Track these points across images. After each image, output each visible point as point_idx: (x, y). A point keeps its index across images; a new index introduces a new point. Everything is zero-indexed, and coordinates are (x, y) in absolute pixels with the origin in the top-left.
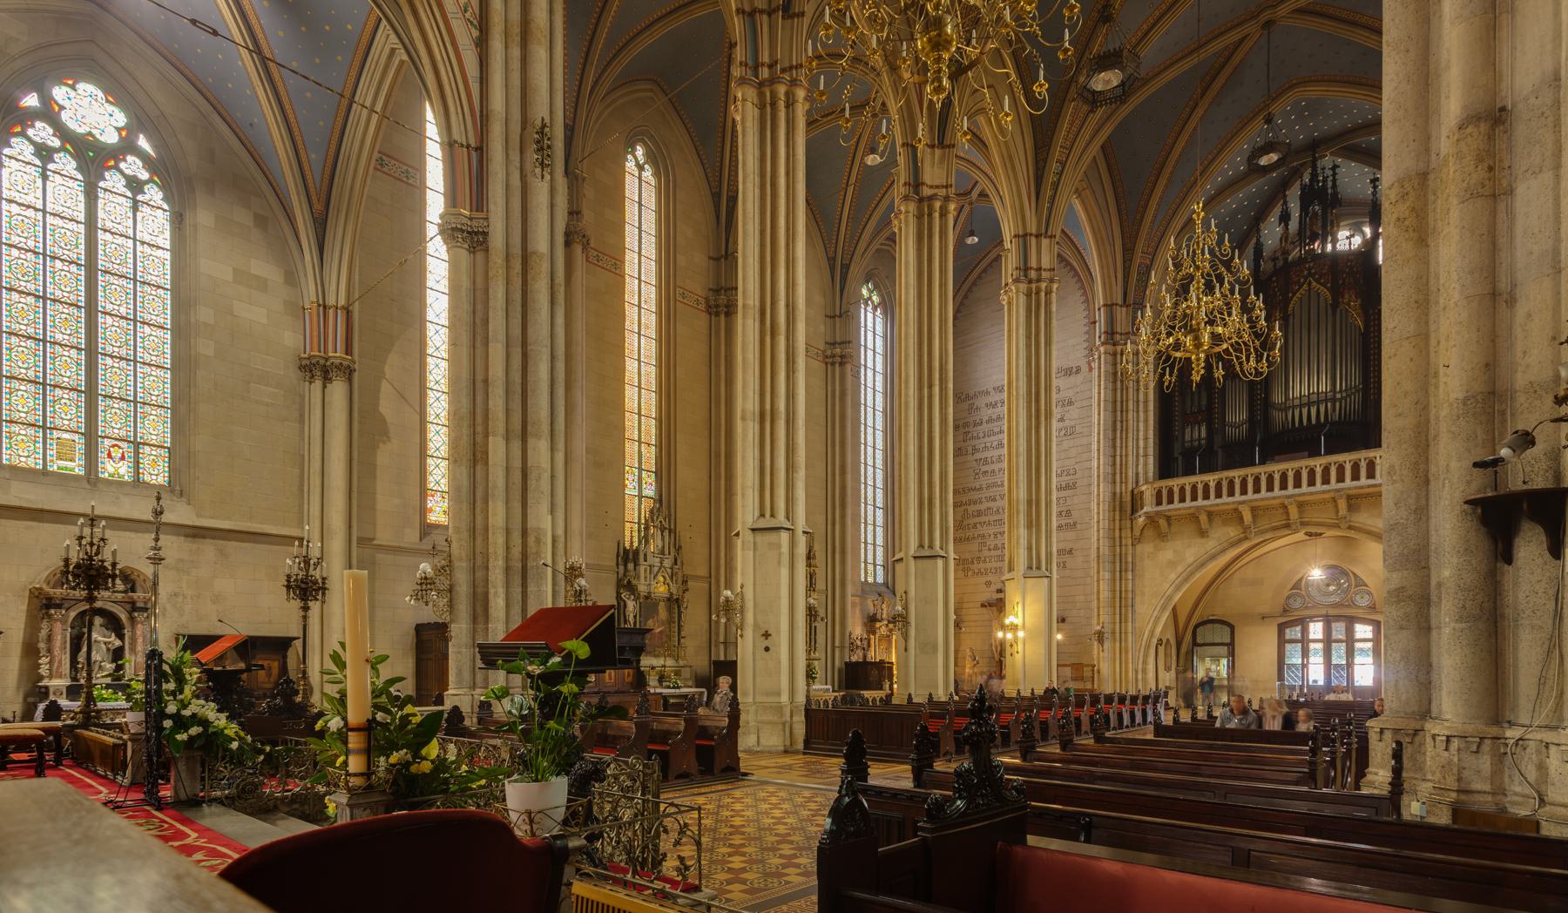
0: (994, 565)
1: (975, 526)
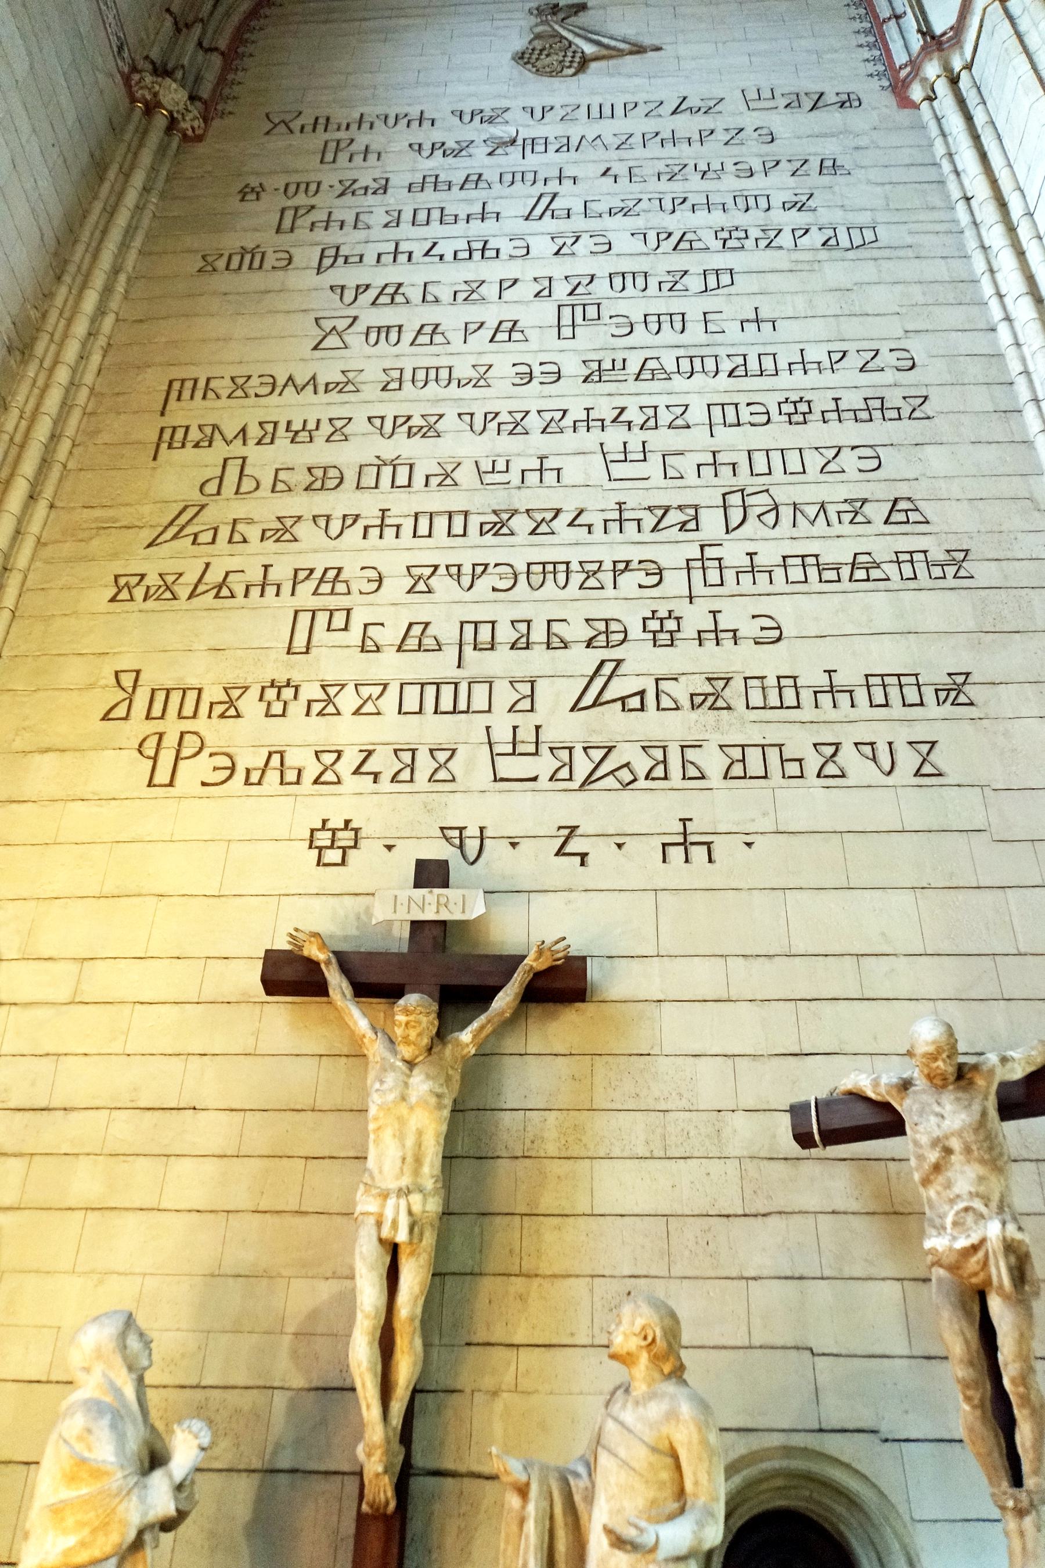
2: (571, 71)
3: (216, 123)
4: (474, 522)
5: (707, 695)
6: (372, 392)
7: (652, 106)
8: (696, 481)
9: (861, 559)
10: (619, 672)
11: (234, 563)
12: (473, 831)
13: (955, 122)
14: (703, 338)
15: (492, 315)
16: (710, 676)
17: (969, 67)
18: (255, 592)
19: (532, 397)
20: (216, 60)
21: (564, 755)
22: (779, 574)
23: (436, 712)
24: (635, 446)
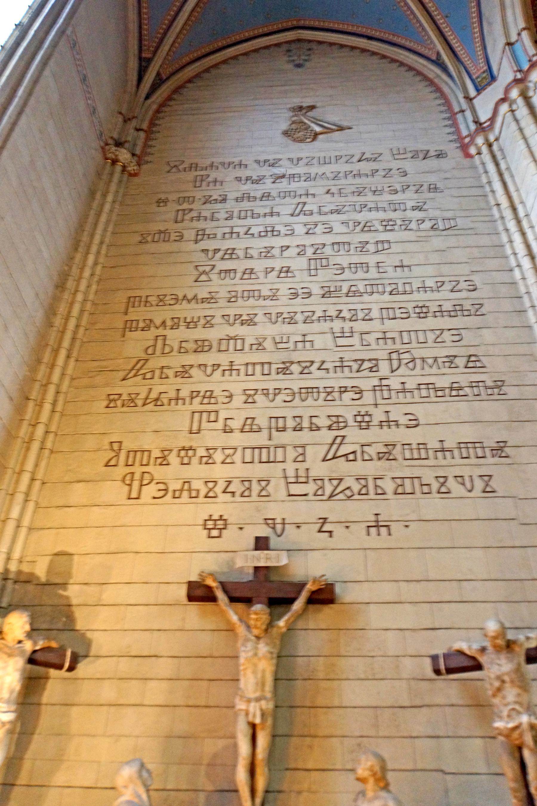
2: (308, 140)
3: (144, 167)
4: (274, 367)
6: (222, 303)
7: (348, 157)
8: (377, 347)
9: (455, 385)
10: (344, 442)
11: (162, 388)
12: (279, 521)
13: (491, 167)
14: (377, 276)
15: (277, 264)
16: (387, 443)
17: (497, 139)
18: (173, 402)
19: (298, 305)
20: (142, 135)
22: (416, 392)
24: (347, 330)
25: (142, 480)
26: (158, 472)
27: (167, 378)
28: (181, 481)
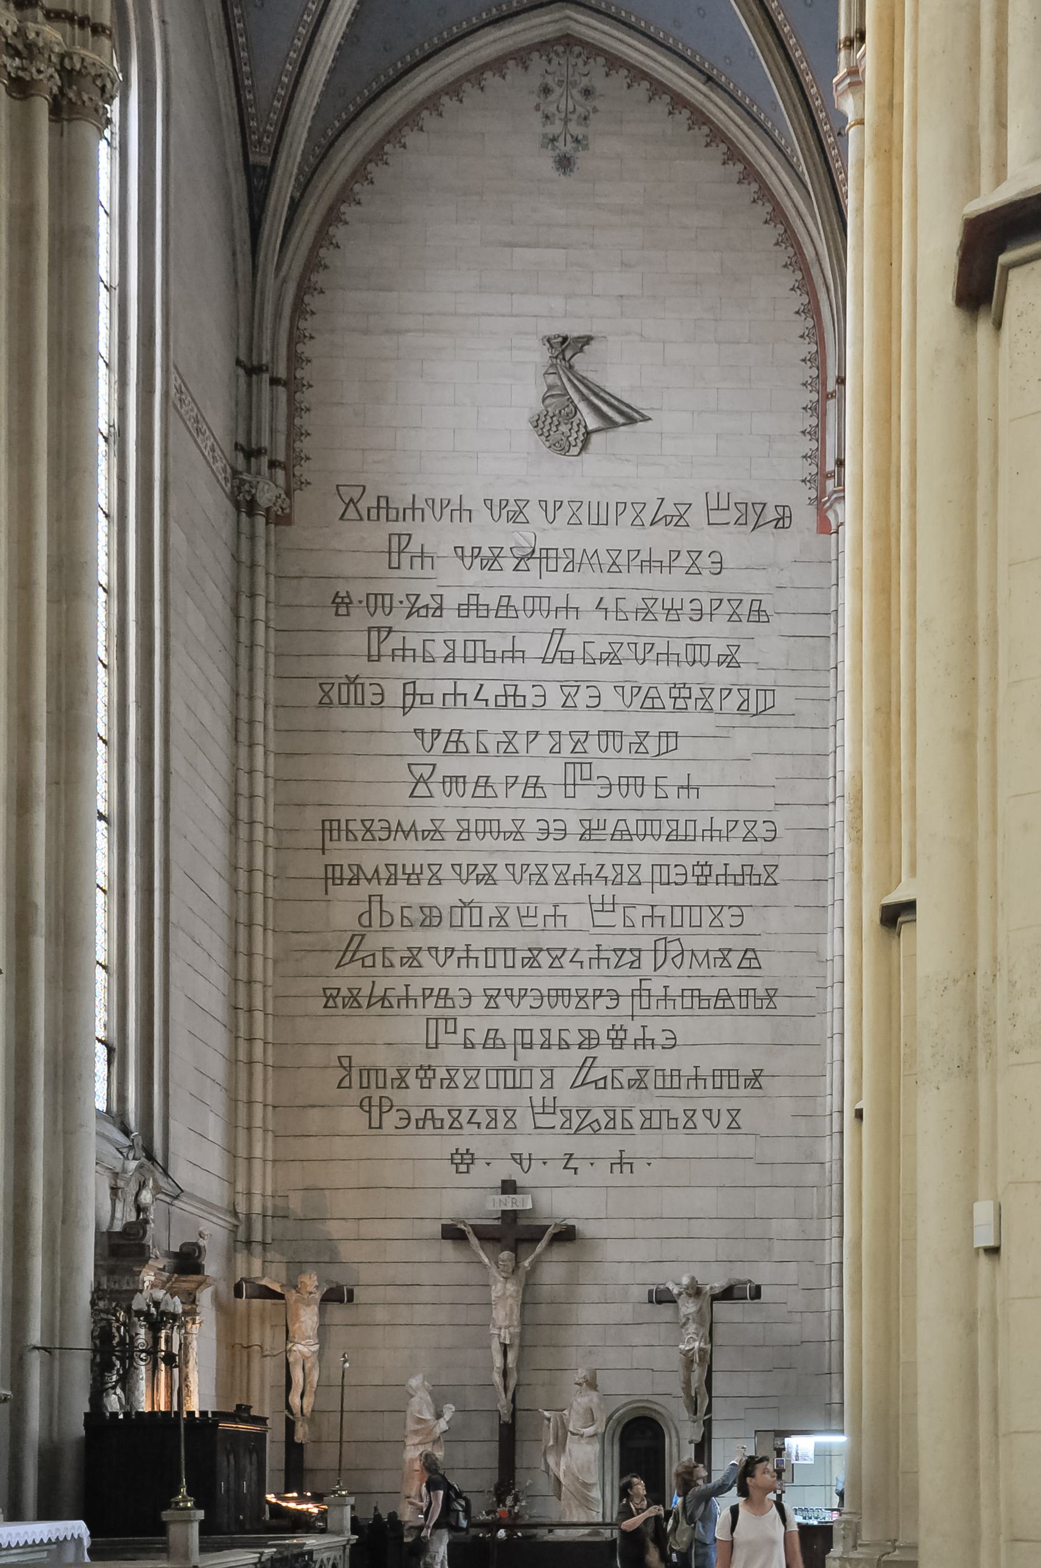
0: (483, 1097)
1: (412, 957)
4: (519, 955)
5: (636, 1080)
6: (451, 840)
12: (526, 1156)
15: (521, 768)
18: (403, 1003)
21: (567, 1114)
23: (505, 1088)
24: (608, 899)
25: (381, 1106)
26: (399, 1097)
27: (392, 966)
28: (423, 1109)
